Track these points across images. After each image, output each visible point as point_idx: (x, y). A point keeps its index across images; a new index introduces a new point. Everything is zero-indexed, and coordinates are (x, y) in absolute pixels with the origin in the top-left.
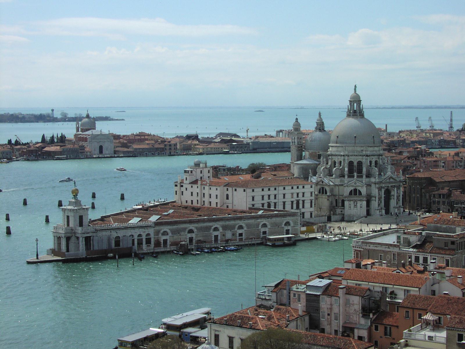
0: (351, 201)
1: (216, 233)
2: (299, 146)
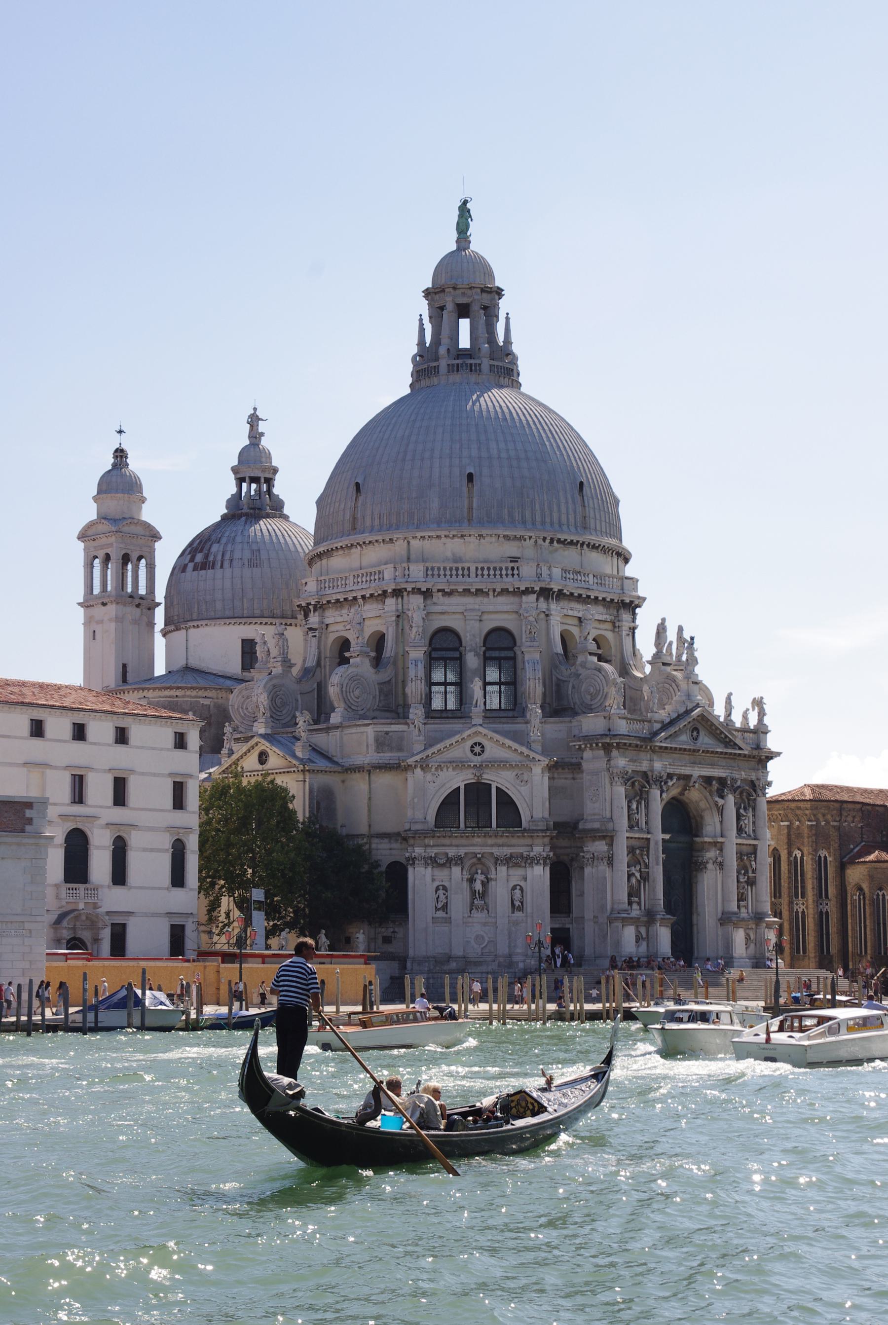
0: (449, 862)
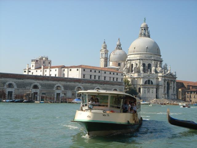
0: (146, 88)
1: (58, 92)
2: (106, 58)
